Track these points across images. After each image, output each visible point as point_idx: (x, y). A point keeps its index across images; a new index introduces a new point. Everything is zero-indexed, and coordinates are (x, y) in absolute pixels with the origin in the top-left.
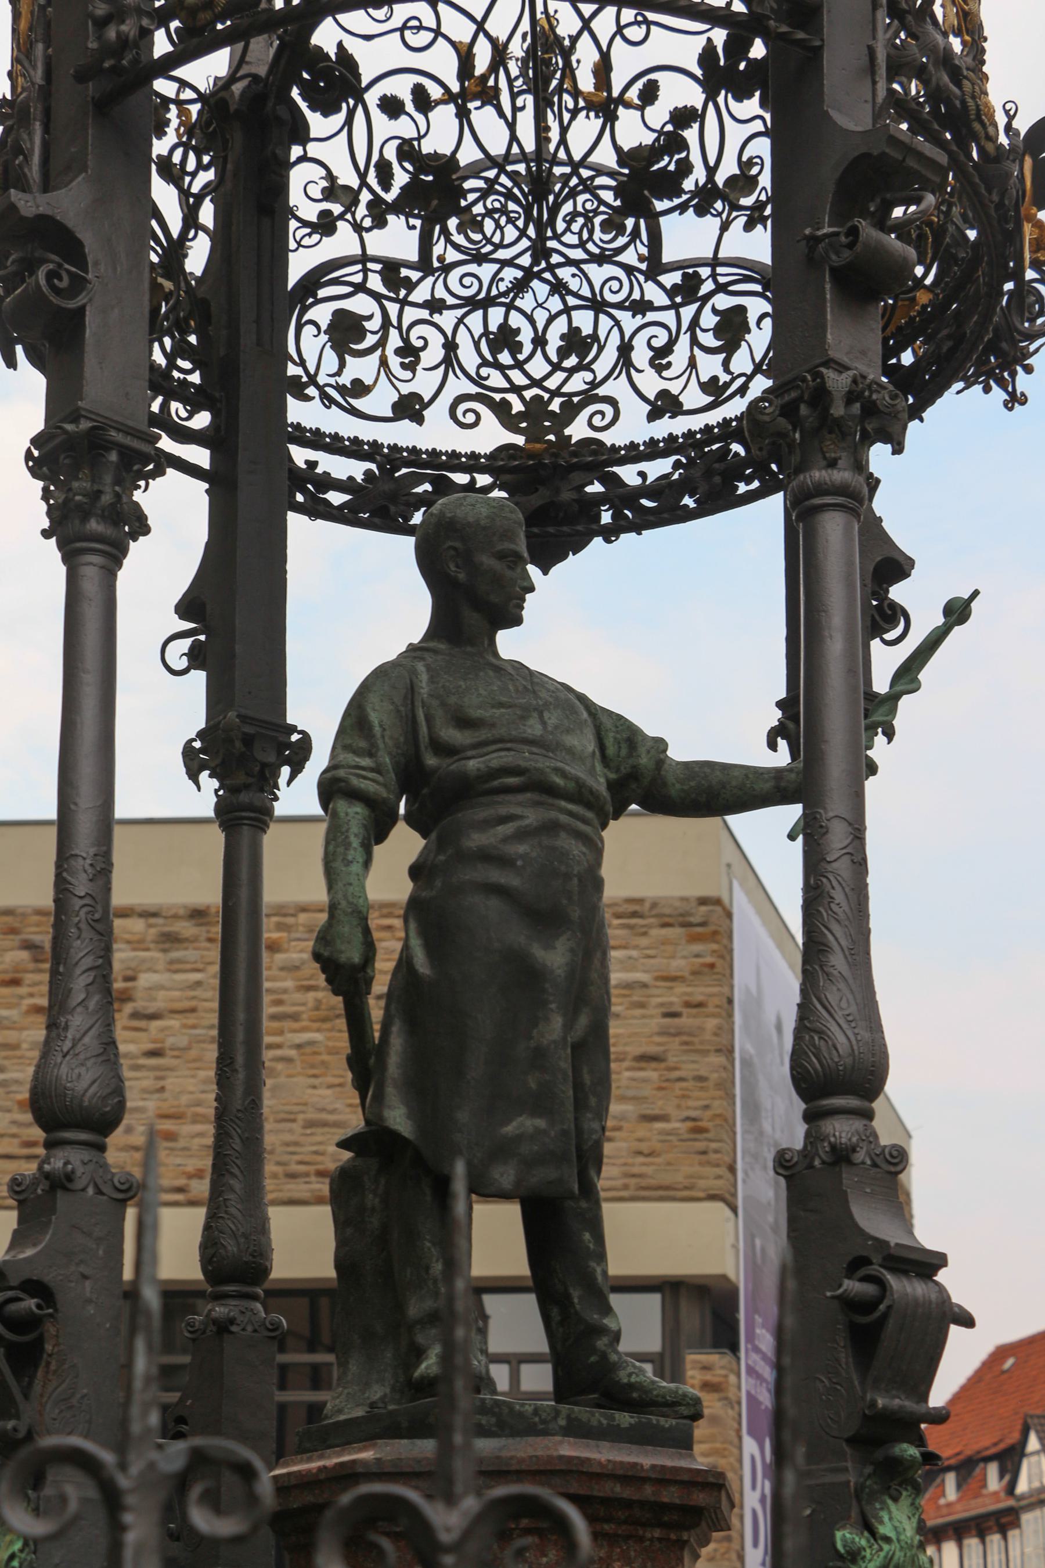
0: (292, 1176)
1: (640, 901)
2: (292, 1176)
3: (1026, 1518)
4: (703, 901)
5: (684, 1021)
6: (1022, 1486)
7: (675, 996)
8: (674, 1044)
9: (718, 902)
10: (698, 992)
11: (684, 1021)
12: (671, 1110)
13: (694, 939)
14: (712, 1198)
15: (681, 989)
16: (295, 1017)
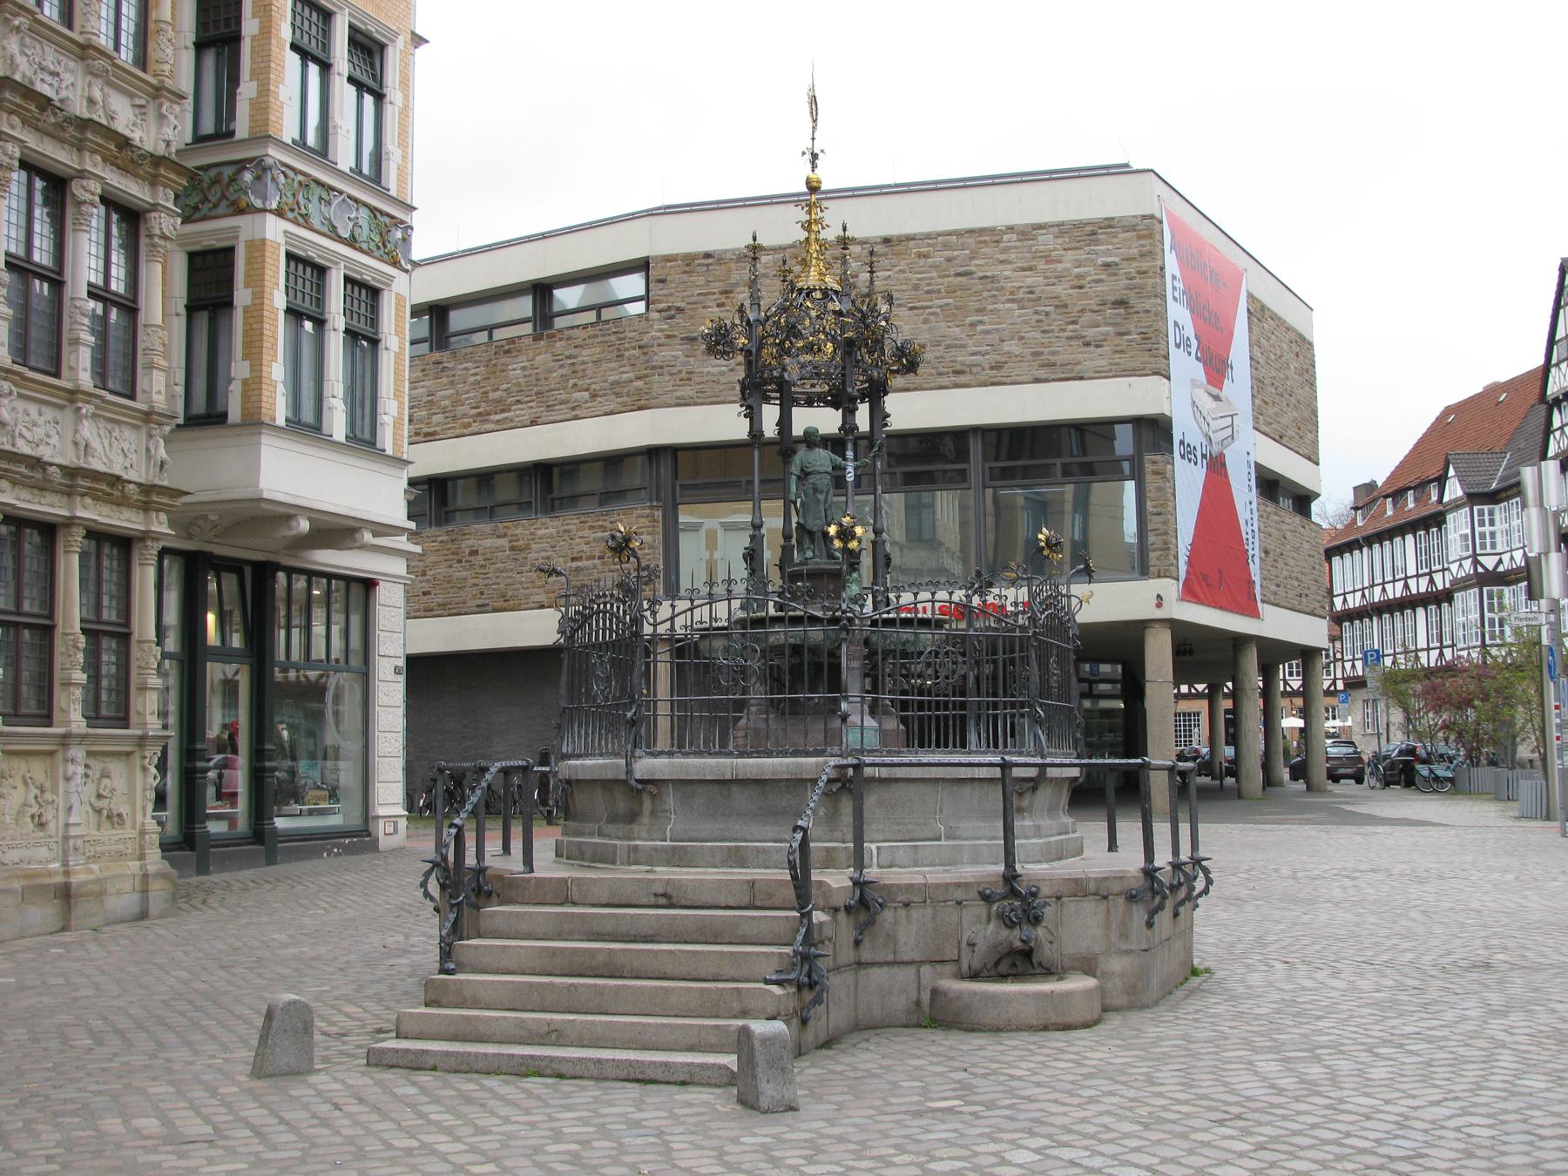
0: (940, 374)
1: (1112, 219)
2: (940, 374)
3: (1449, 517)
4: (1145, 217)
5: (1137, 281)
6: (1446, 499)
7: (1131, 269)
8: (1132, 294)
9: (1152, 217)
10: (1144, 265)
11: (1137, 281)
12: (1132, 328)
13: (1140, 237)
14: (1155, 374)
15: (1135, 264)
16: (939, 291)
